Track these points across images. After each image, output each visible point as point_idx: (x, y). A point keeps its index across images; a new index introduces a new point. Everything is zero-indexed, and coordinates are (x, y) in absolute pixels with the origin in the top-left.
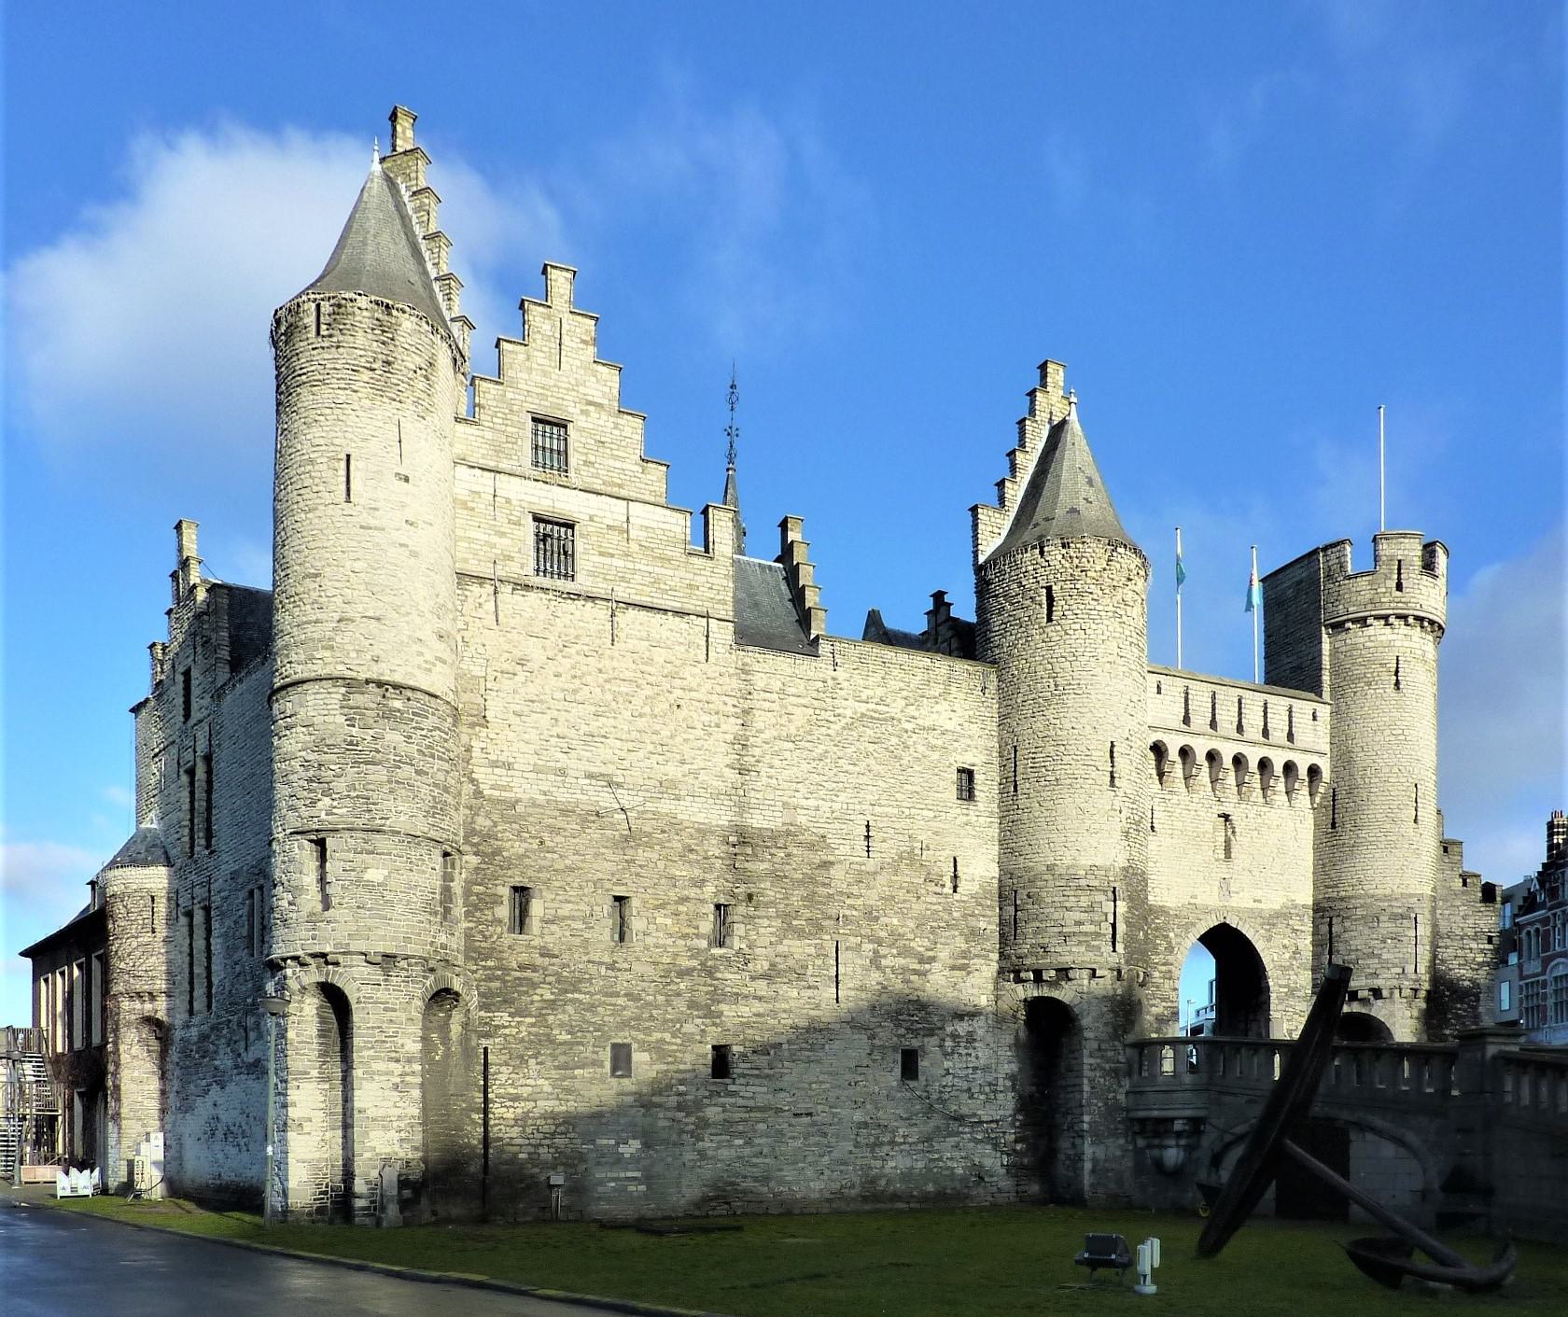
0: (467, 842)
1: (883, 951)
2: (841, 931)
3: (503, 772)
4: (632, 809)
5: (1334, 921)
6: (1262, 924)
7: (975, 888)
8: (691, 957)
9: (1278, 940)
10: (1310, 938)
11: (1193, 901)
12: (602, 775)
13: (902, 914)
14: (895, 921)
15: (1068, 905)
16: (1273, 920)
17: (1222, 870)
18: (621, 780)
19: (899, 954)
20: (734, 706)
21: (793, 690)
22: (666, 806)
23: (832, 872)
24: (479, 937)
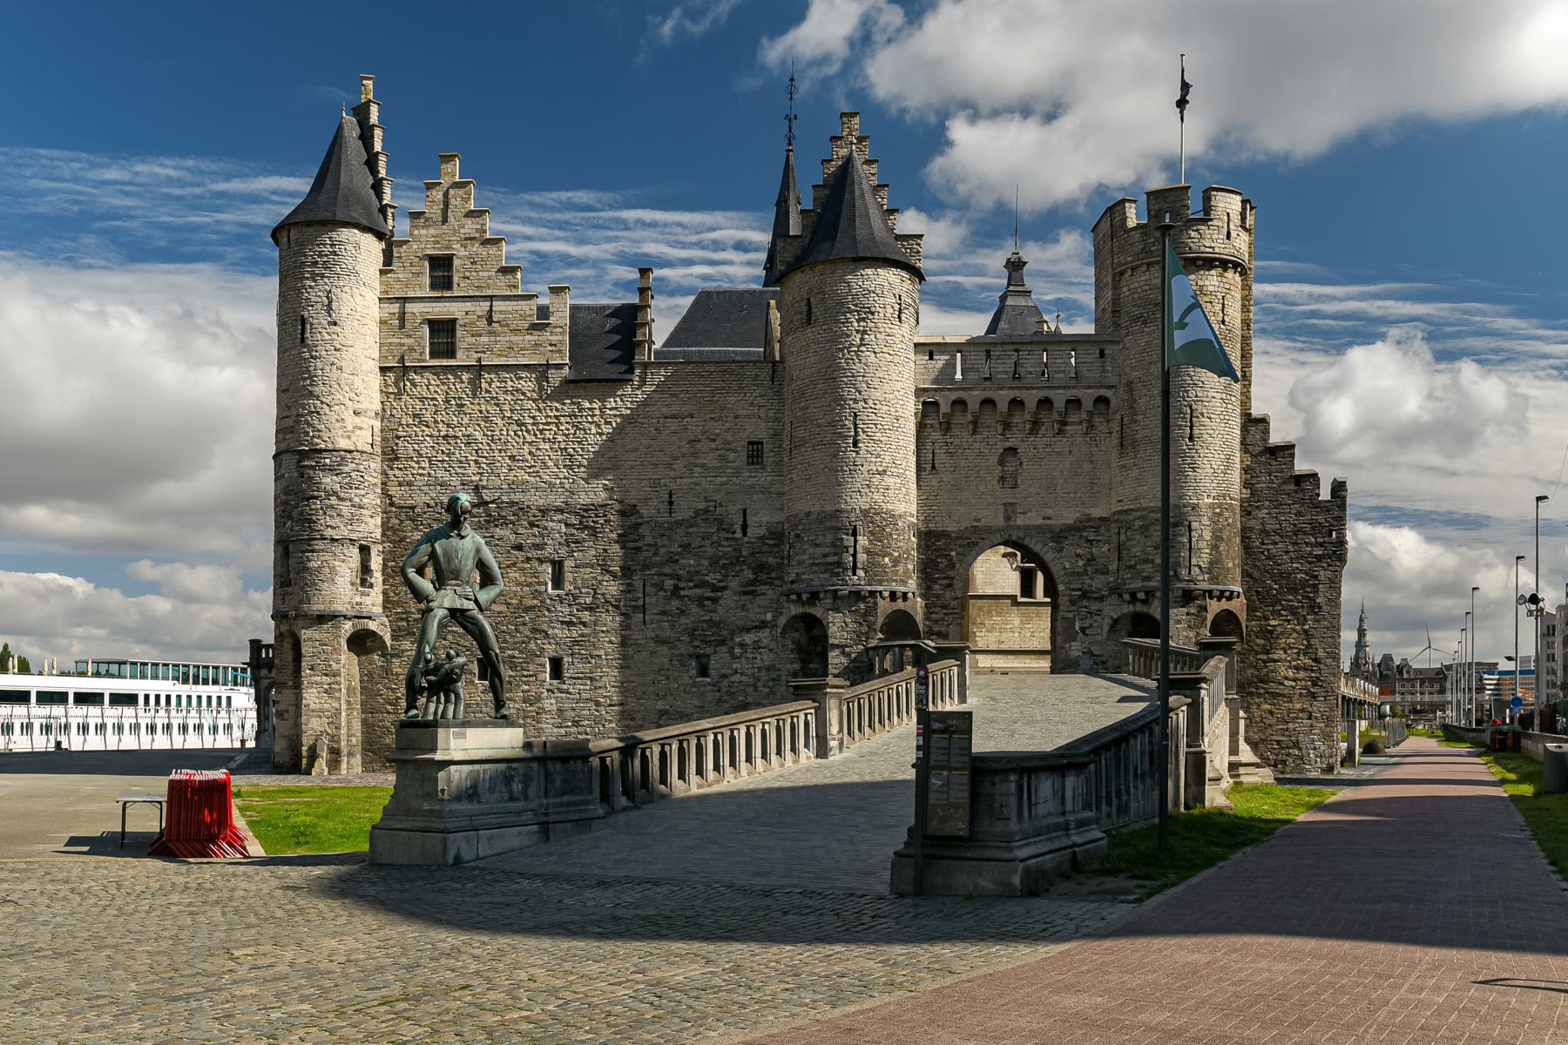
0: (383, 535)
1: (681, 585)
2: (648, 572)
3: (407, 488)
4: (492, 502)
5: (1121, 531)
6: (1052, 539)
7: (762, 532)
8: (534, 598)
9: (1069, 550)
10: (1107, 546)
11: (975, 524)
12: (472, 481)
13: (698, 556)
14: (692, 562)
15: (818, 542)
16: (1059, 536)
17: (1008, 496)
18: (485, 483)
19: (695, 586)
20: (567, 423)
21: (614, 405)
22: (516, 497)
23: (641, 530)
24: (392, 595)
